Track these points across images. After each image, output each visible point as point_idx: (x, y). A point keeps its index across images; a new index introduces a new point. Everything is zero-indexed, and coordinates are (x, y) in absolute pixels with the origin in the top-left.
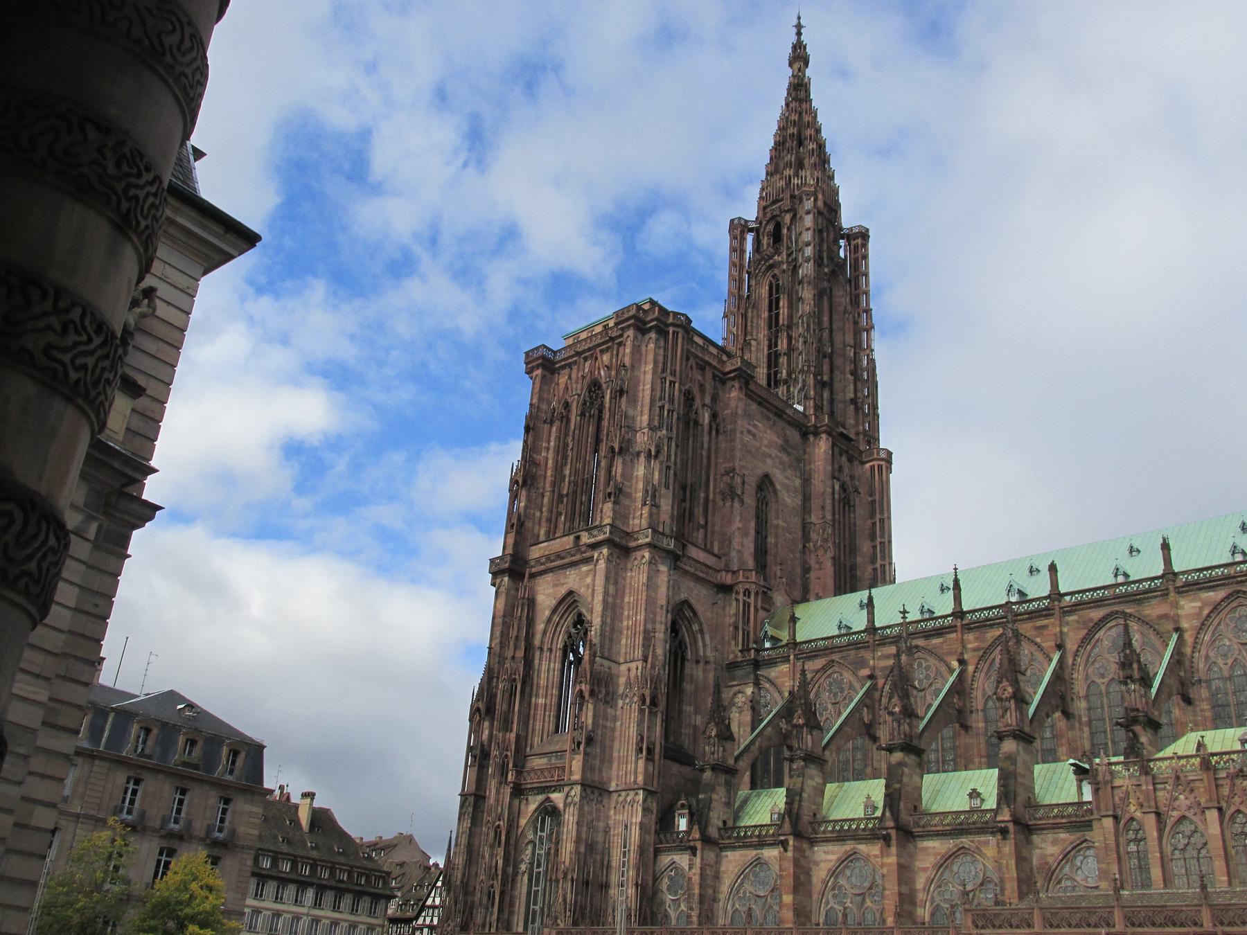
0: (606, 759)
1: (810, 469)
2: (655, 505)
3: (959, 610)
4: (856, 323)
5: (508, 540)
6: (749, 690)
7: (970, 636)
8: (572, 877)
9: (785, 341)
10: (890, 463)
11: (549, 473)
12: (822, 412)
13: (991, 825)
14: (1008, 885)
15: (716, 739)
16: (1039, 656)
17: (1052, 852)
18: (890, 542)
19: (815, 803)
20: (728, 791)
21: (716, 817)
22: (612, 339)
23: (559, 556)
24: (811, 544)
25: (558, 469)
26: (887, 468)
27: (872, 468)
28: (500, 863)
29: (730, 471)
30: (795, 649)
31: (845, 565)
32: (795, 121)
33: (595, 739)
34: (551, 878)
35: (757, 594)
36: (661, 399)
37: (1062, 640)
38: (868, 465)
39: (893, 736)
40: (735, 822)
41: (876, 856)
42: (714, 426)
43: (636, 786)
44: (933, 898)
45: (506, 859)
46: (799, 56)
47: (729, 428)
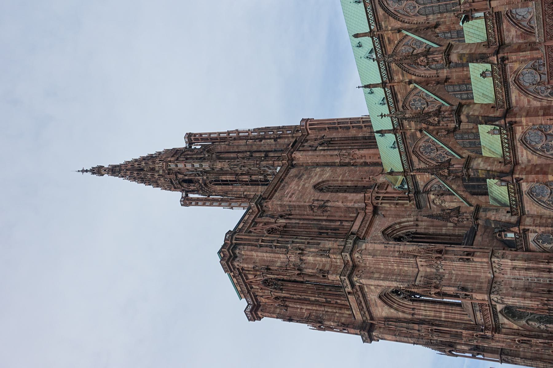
0: (475, 279)
3: (381, 85)
4: (235, 139)
5: (352, 332)
6: (432, 197)
7: (396, 78)
8: (546, 300)
9: (244, 177)
10: (309, 119)
11: (314, 308)
12: (280, 156)
13: (500, 66)
14: (535, 56)
15: (459, 217)
16: (406, 41)
17: (515, 32)
18: (350, 119)
19: (493, 163)
20: (490, 210)
21: (505, 217)
22: (240, 274)
23: (359, 304)
24: (351, 162)
25: (312, 303)
26: (310, 121)
27: (310, 129)
28: (541, 340)
29: (311, 207)
30: (407, 172)
31: (364, 142)
32: (130, 173)
33: (463, 286)
34: (547, 313)
35: (377, 193)
37: (395, 30)
38: (310, 132)
39: (452, 120)
40: (508, 206)
41: (523, 128)
42: (287, 216)
44: (546, 96)
45: (538, 337)
46: (98, 171)
47: (288, 208)
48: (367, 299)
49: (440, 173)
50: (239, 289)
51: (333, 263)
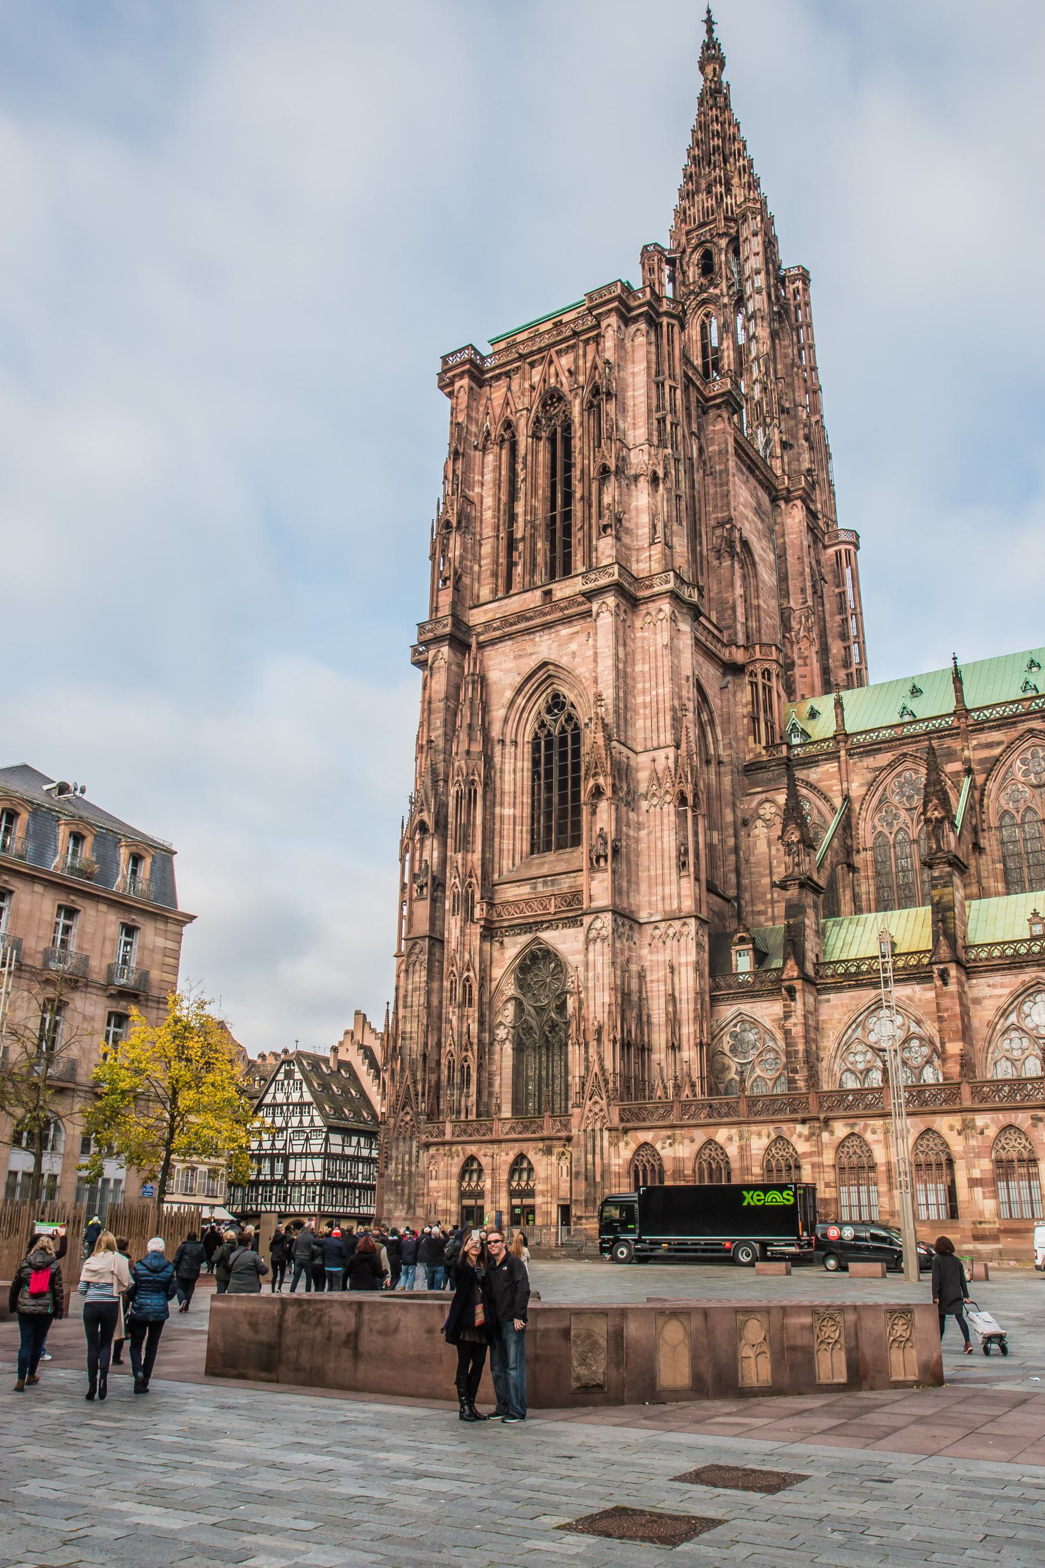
1: (784, 542)
2: (668, 545)
5: (440, 599)
8: (615, 1037)
15: (801, 846)
22: (576, 334)
23: (521, 616)
27: (838, 554)
28: (474, 1028)
30: (846, 742)
35: (777, 675)
36: (658, 410)
38: (831, 551)
43: (682, 915)
45: (481, 1023)
47: (717, 468)
48: (538, 634)
49: (931, 801)
50: (543, 328)
51: (634, 553)
